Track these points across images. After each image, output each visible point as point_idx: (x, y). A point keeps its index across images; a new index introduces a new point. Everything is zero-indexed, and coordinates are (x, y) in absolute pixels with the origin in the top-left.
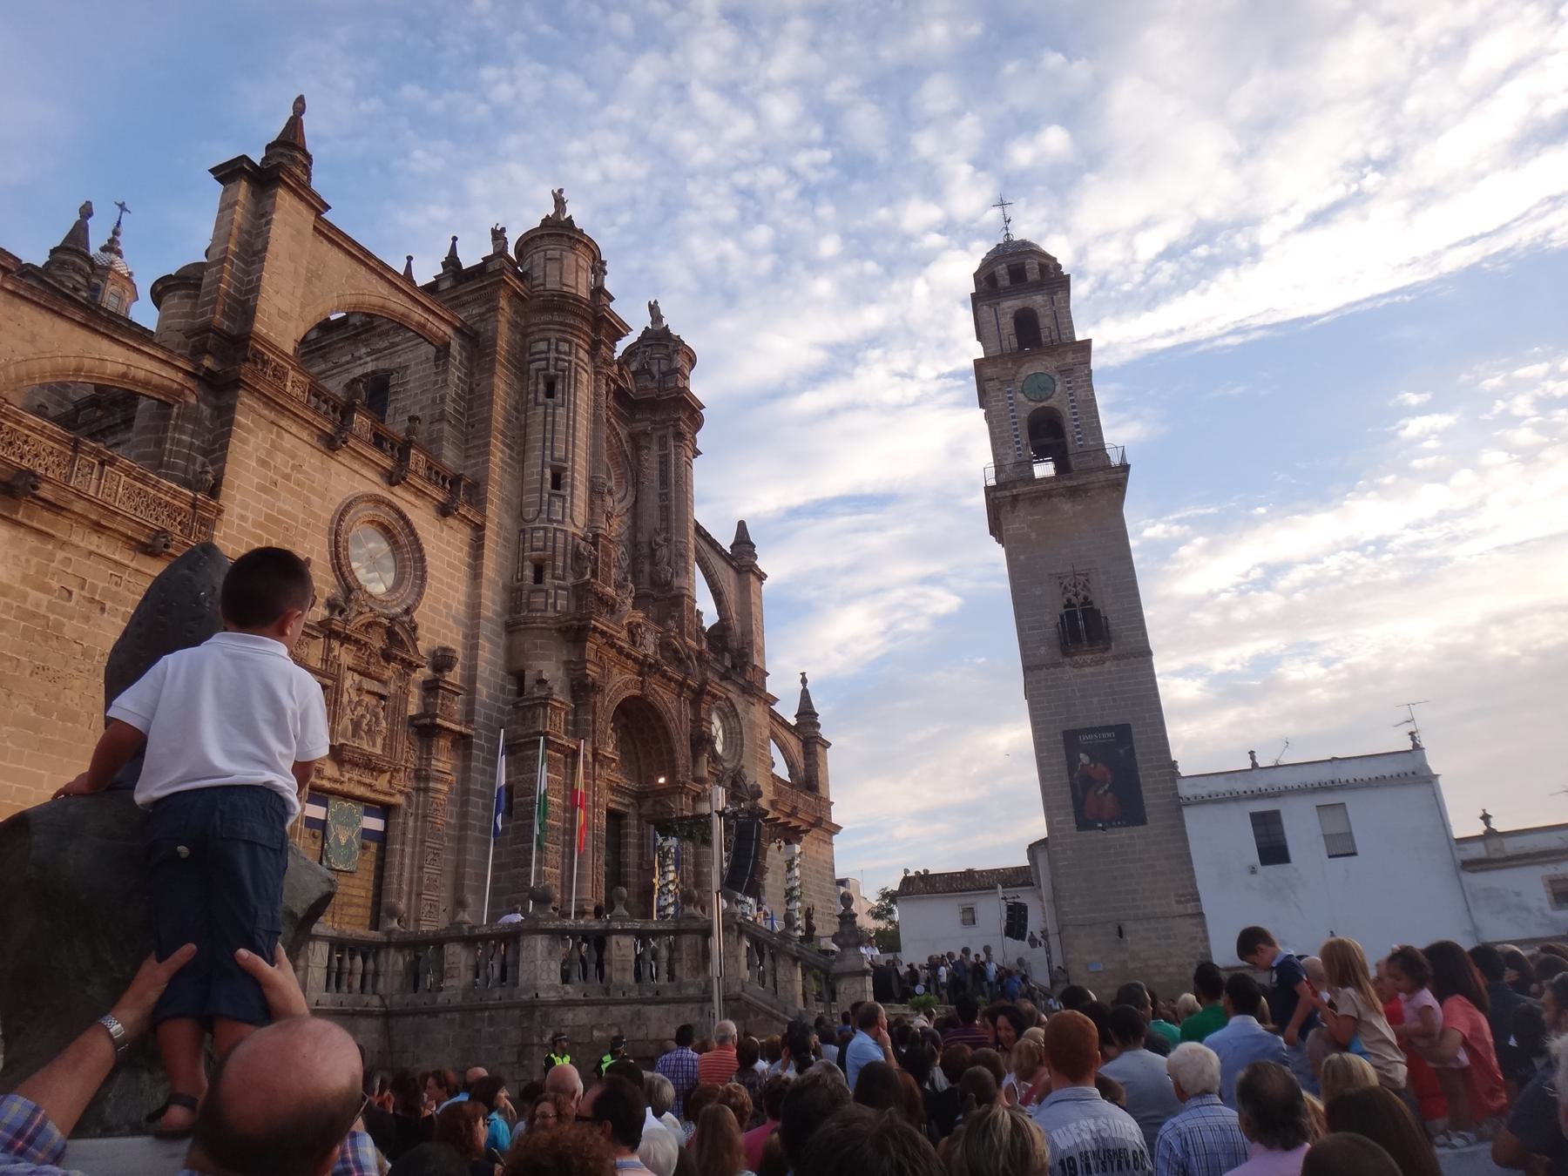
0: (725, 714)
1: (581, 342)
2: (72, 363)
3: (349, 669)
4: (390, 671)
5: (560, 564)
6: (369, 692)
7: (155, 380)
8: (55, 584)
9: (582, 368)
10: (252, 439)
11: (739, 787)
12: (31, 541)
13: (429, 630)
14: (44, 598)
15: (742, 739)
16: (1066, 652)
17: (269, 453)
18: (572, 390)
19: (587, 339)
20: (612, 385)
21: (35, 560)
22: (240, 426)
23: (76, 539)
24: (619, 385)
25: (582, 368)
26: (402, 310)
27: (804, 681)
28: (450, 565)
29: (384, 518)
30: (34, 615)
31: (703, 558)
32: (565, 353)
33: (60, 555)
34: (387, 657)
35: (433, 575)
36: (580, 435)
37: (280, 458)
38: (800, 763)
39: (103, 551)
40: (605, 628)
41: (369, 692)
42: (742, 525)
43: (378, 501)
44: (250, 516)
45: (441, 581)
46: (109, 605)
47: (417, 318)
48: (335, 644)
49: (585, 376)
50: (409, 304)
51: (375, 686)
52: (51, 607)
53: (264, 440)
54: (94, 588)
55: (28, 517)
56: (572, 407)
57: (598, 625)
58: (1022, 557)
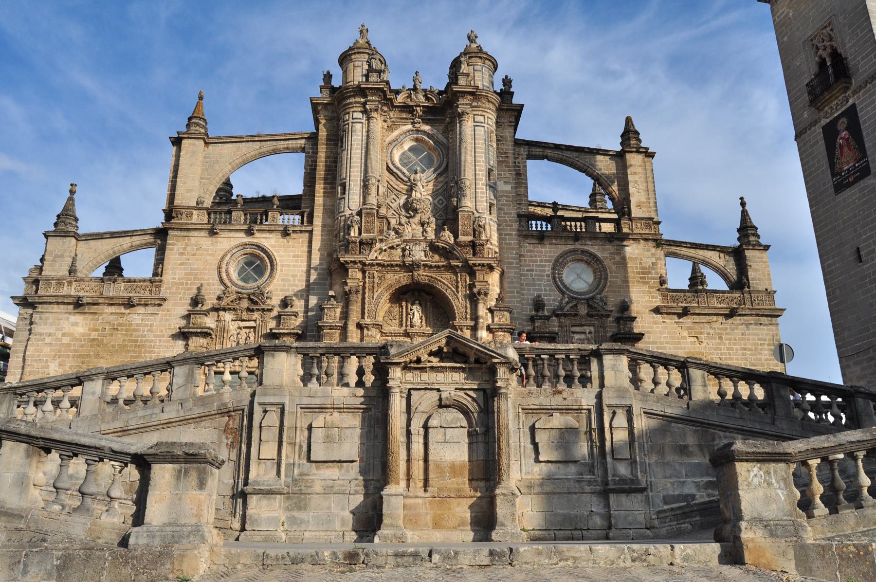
0: (586, 262)
1: (355, 109)
2: (111, 252)
3: (232, 320)
4: (256, 315)
5: (342, 234)
6: (245, 328)
7: (143, 242)
8: (100, 328)
9: (357, 122)
10: (175, 247)
11: (595, 308)
12: (91, 317)
13: (282, 290)
14: (97, 333)
15: (606, 274)
16: (819, 109)
17: (185, 249)
18: (350, 138)
19: (357, 105)
20: (418, 109)
21: (92, 322)
22: (170, 244)
23: (106, 311)
24: (423, 106)
25: (357, 122)
26: (272, 148)
27: (743, 204)
28: (294, 256)
29: (249, 250)
30: (94, 340)
31: (572, 162)
32: (347, 120)
33: (101, 318)
34: (253, 311)
35: (282, 266)
36: (355, 160)
37: (189, 248)
38: (731, 268)
39: (118, 311)
40: (352, 259)
41: (245, 328)
42: (628, 120)
43: (244, 245)
44: (177, 277)
45: (289, 266)
46: (119, 328)
47: (282, 147)
48: (222, 313)
49: (358, 126)
50: (275, 143)
51: (252, 324)
52: (99, 335)
53: (182, 245)
54: (114, 324)
55: (89, 310)
56: (349, 147)
57: (346, 259)
58: (785, 39)
